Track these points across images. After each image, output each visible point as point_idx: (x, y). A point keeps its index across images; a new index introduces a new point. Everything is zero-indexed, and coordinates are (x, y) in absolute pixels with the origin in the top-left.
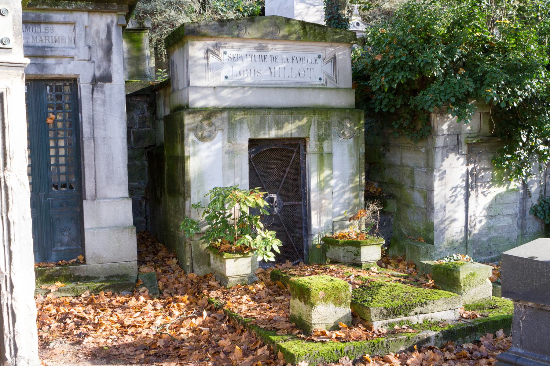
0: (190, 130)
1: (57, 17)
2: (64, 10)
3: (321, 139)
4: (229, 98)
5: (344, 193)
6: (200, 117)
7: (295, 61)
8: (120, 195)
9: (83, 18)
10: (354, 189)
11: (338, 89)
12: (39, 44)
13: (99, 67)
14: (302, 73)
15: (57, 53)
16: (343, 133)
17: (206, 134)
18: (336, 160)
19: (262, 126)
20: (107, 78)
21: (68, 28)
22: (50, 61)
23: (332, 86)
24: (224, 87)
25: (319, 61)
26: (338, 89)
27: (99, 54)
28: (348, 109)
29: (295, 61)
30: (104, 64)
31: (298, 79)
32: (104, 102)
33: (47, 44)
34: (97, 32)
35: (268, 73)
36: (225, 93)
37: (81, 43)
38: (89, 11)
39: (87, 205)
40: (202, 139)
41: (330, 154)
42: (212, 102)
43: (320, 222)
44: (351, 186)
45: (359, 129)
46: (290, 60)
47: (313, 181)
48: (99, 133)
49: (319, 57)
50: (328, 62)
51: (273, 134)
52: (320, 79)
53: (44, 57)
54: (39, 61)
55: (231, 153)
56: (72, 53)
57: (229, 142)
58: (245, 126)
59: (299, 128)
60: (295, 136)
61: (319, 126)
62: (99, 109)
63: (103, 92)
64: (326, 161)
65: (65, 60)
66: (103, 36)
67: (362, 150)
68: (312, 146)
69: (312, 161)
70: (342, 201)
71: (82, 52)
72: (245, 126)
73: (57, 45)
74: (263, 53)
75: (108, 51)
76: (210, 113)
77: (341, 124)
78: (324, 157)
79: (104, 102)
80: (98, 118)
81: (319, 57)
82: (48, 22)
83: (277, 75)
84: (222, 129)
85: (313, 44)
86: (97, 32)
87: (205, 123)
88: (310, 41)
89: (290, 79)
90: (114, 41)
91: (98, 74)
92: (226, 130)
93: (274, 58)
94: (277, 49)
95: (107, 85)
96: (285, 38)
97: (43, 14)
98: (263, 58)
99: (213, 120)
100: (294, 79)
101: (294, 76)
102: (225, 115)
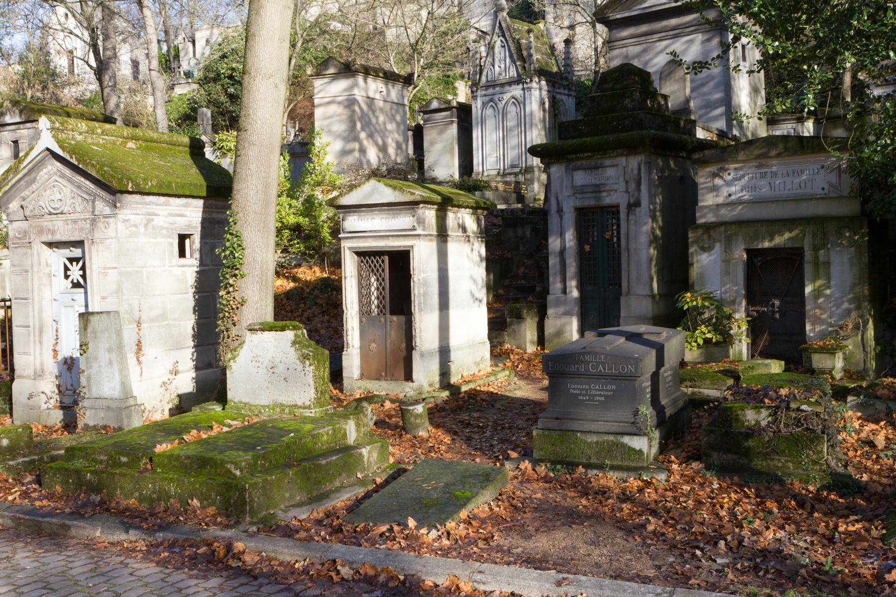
0: (693, 242)
1: (608, 162)
2: (610, 157)
3: (816, 249)
4: (726, 214)
5: (842, 303)
6: (700, 232)
7: (796, 174)
8: (645, 293)
9: (622, 160)
10: (850, 301)
11: (841, 197)
12: (598, 183)
13: (633, 196)
14: (803, 185)
15: (607, 188)
16: (841, 243)
17: (706, 246)
18: (835, 269)
19: (756, 237)
20: (638, 204)
21: (615, 168)
22: (604, 194)
23: (834, 195)
24: (723, 205)
25: (822, 171)
26: (841, 197)
27: (633, 186)
28: (848, 217)
29: (796, 174)
30: (636, 194)
31: (799, 191)
32: (636, 222)
33: (602, 182)
34: (632, 170)
35: (768, 188)
36: (723, 211)
37: (621, 179)
38: (626, 155)
39: (623, 300)
40: (704, 249)
41: (828, 264)
42: (711, 218)
43: (813, 330)
44: (851, 296)
45: (862, 237)
46: (791, 174)
47: (808, 289)
48: (632, 246)
49: (823, 167)
50: (832, 171)
51: (766, 244)
52: (823, 189)
53: (600, 192)
54: (598, 195)
55: (727, 261)
56: (615, 187)
57: (726, 252)
58: (740, 238)
59: (790, 239)
60: (789, 245)
61: (814, 236)
62: (632, 227)
63: (635, 214)
64: (821, 271)
65: (612, 193)
66: (636, 172)
67: (865, 259)
68: (808, 255)
69: (808, 269)
70: (839, 311)
71: (622, 186)
72: (740, 238)
73: (608, 182)
74: (763, 170)
75: (639, 184)
76: (708, 228)
77: (840, 235)
78: (822, 269)
79: (636, 222)
80: (632, 234)
81: (823, 167)
82: (603, 167)
83: (777, 188)
84: (720, 241)
85: (813, 156)
86: (632, 170)
87: (705, 236)
88: (809, 154)
89: (791, 192)
90: (642, 175)
91: (632, 201)
92: (723, 241)
93: (774, 174)
94: (775, 166)
95: (638, 209)
96: (778, 155)
97: (599, 161)
98: (763, 176)
99: (712, 233)
100: (795, 191)
101: (794, 188)
102: (723, 228)
